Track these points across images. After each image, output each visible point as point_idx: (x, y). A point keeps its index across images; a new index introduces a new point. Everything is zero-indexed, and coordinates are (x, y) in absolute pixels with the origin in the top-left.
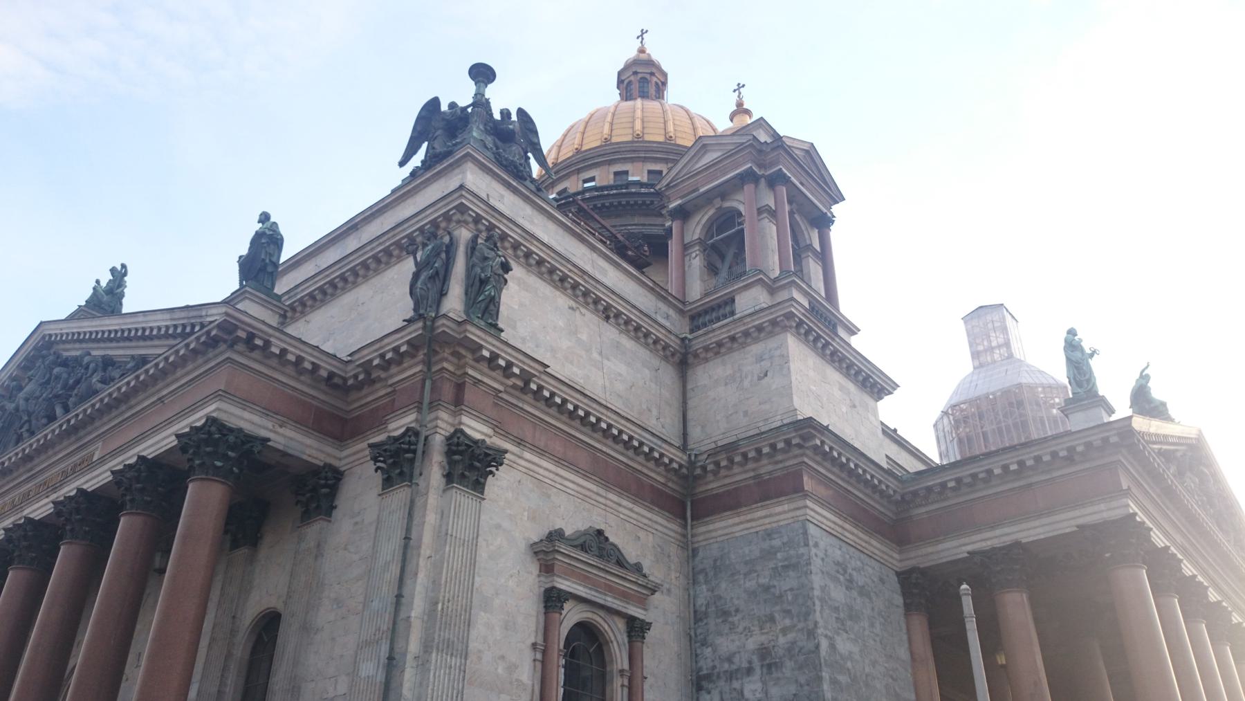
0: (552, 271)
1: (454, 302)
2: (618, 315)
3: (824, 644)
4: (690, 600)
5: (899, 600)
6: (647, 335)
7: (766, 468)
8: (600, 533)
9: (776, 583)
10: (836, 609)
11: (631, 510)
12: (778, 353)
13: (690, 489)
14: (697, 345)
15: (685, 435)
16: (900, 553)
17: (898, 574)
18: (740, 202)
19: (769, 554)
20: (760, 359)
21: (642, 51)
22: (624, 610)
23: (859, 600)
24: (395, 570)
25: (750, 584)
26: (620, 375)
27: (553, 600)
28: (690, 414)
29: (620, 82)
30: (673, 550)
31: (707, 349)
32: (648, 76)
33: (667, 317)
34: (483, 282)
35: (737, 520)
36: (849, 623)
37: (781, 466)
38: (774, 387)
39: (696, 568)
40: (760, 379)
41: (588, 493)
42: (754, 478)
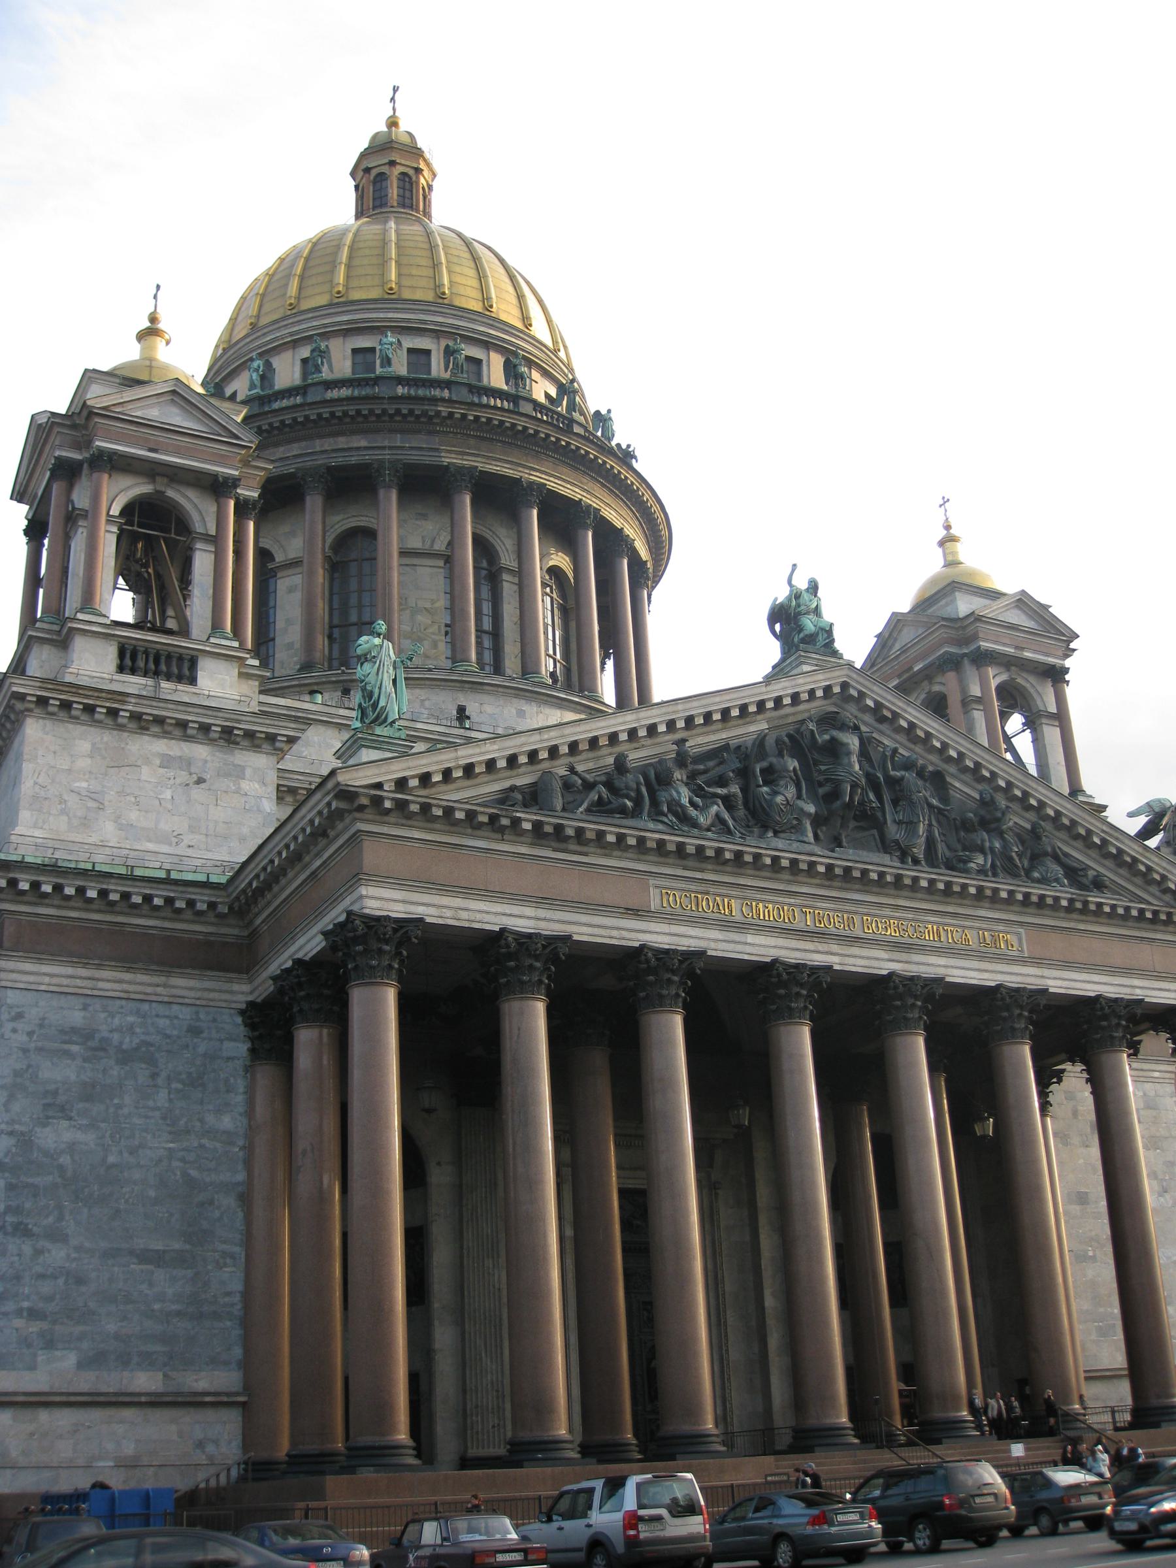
10: (55, 1093)
16: (250, 981)
17: (242, 1013)
21: (393, 123)
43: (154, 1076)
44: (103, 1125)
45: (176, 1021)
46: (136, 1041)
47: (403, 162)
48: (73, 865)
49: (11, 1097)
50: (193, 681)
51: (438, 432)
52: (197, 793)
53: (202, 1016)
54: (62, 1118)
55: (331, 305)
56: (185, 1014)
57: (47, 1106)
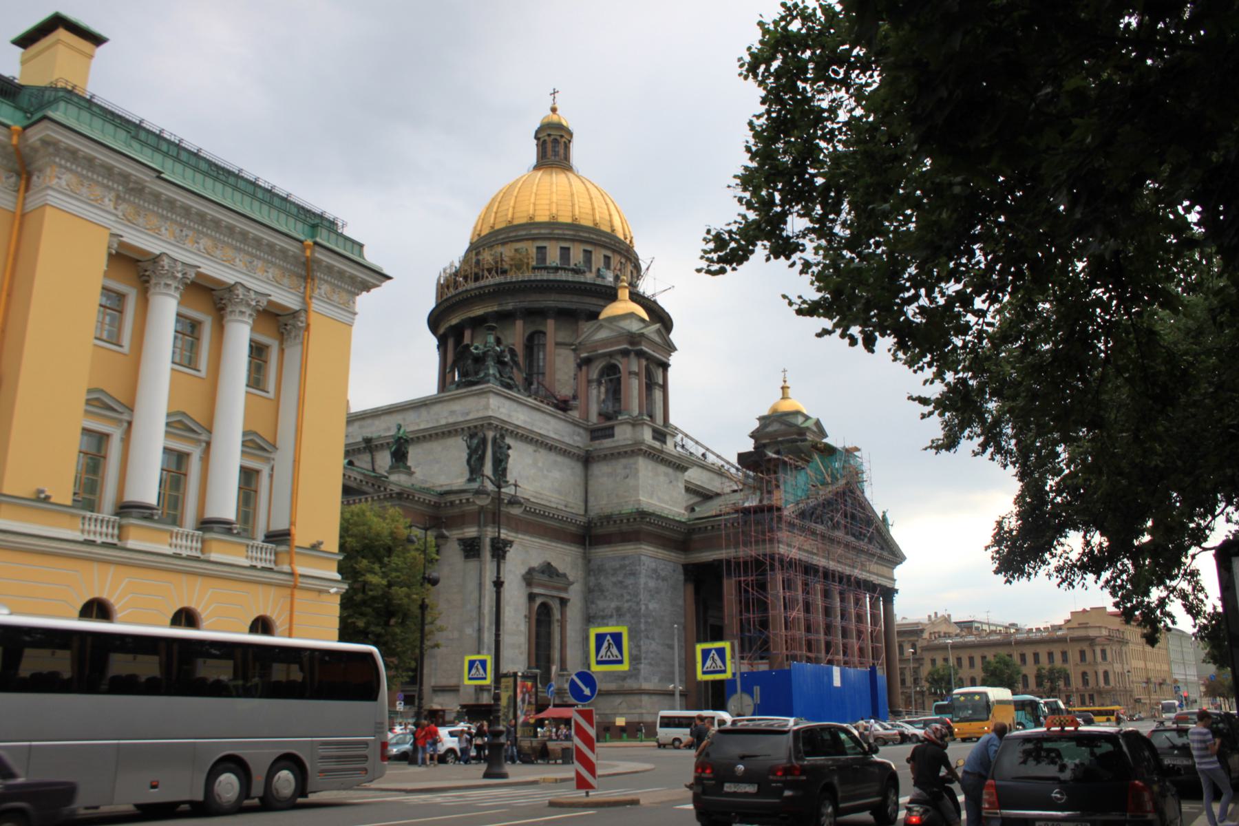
1: (488, 469)
3: (643, 607)
4: (586, 584)
5: (682, 577)
7: (625, 528)
8: (549, 564)
13: (590, 534)
14: (595, 454)
15: (586, 501)
18: (622, 363)
19: (623, 567)
20: (625, 468)
24: (476, 594)
25: (614, 579)
27: (531, 597)
28: (590, 489)
30: (580, 561)
33: (579, 434)
34: (501, 461)
39: (590, 569)
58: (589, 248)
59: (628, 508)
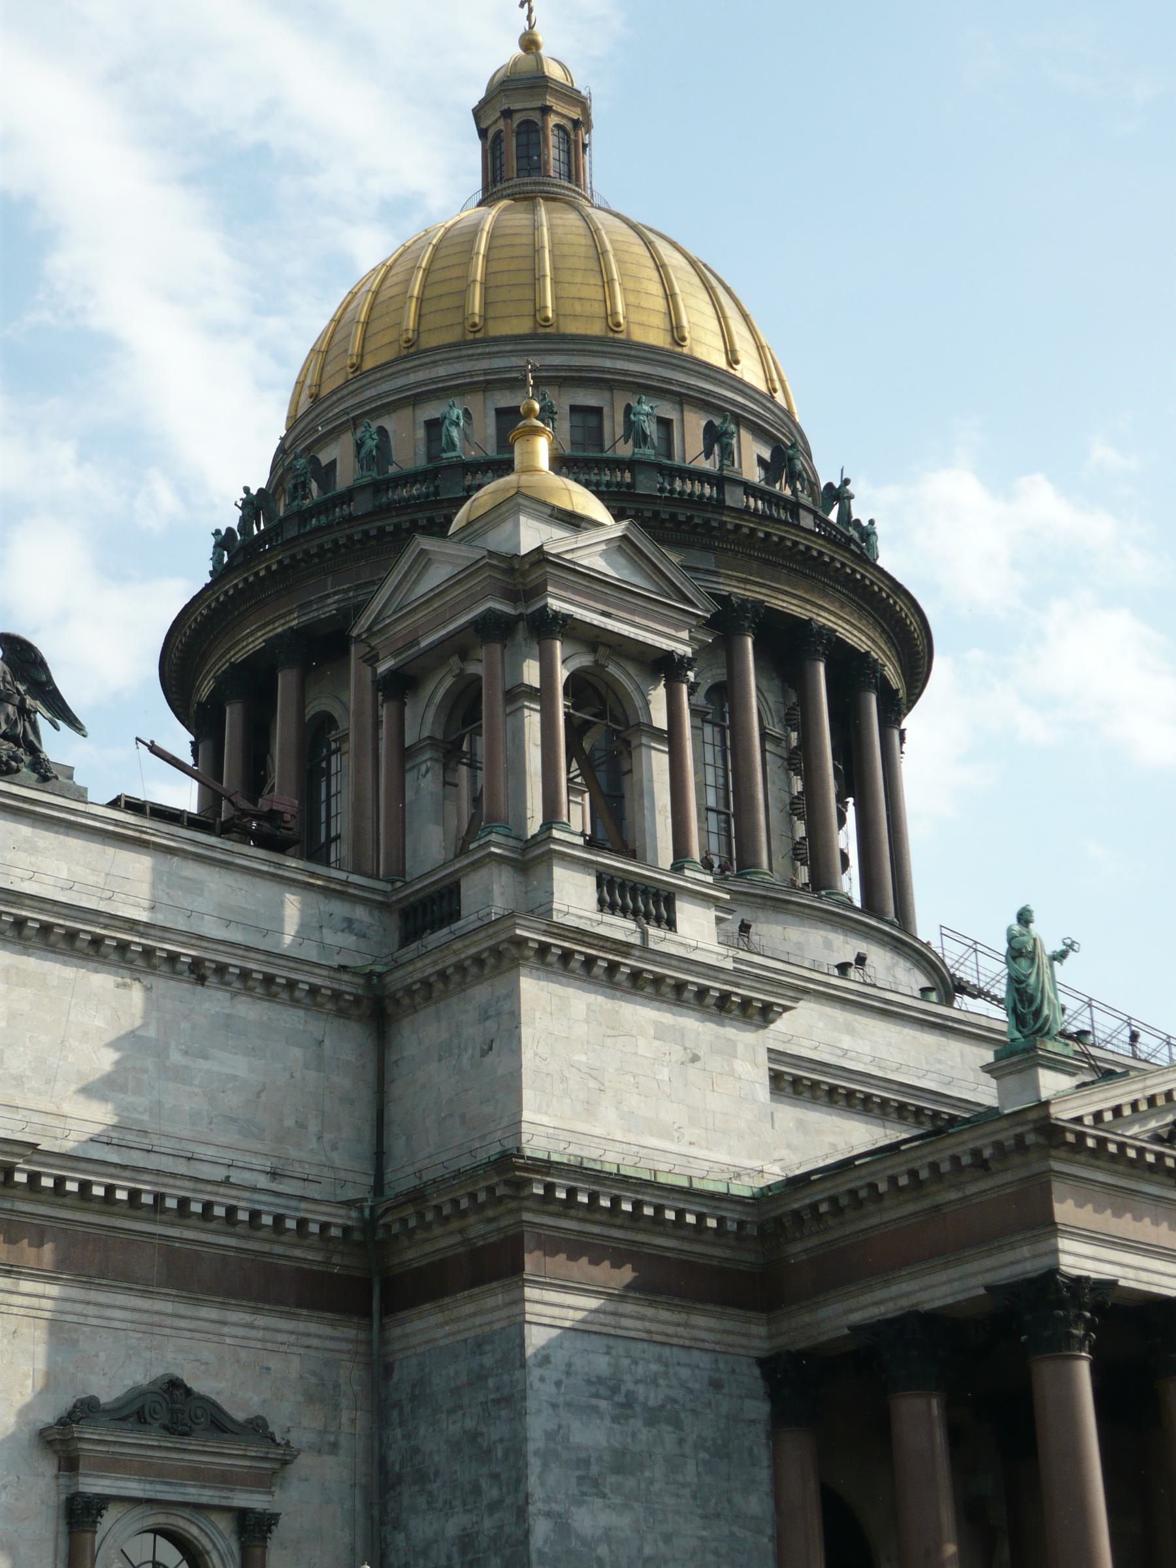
0: (72, 936)
2: (221, 969)
3: (541, 1530)
5: (759, 1409)
6: (291, 985)
7: (478, 1230)
8: (174, 1385)
9: (484, 1430)
10: (587, 1462)
11: (251, 1326)
12: (506, 1006)
15: (380, 1156)
17: (761, 1362)
19: (479, 1378)
20: (485, 1017)
21: (529, 43)
22: (224, 1503)
23: (645, 1434)
25: (453, 1428)
26: (234, 1078)
28: (395, 1112)
29: (482, 133)
31: (409, 991)
32: (535, 117)
33: (349, 925)
35: (440, 1318)
36: (612, 1479)
37: (494, 1225)
38: (500, 1072)
40: (484, 1054)
41: (156, 1319)
42: (461, 1243)
43: (681, 1442)
44: (636, 1505)
45: (697, 1371)
46: (661, 1396)
47: (560, 109)
48: (598, 1167)
49: (545, 1465)
50: (671, 924)
51: (714, 548)
52: (693, 1071)
53: (721, 1365)
54: (596, 1495)
55: (533, 337)
56: (705, 1361)
57: (581, 1479)
58: (588, 398)
59: (482, 1156)
